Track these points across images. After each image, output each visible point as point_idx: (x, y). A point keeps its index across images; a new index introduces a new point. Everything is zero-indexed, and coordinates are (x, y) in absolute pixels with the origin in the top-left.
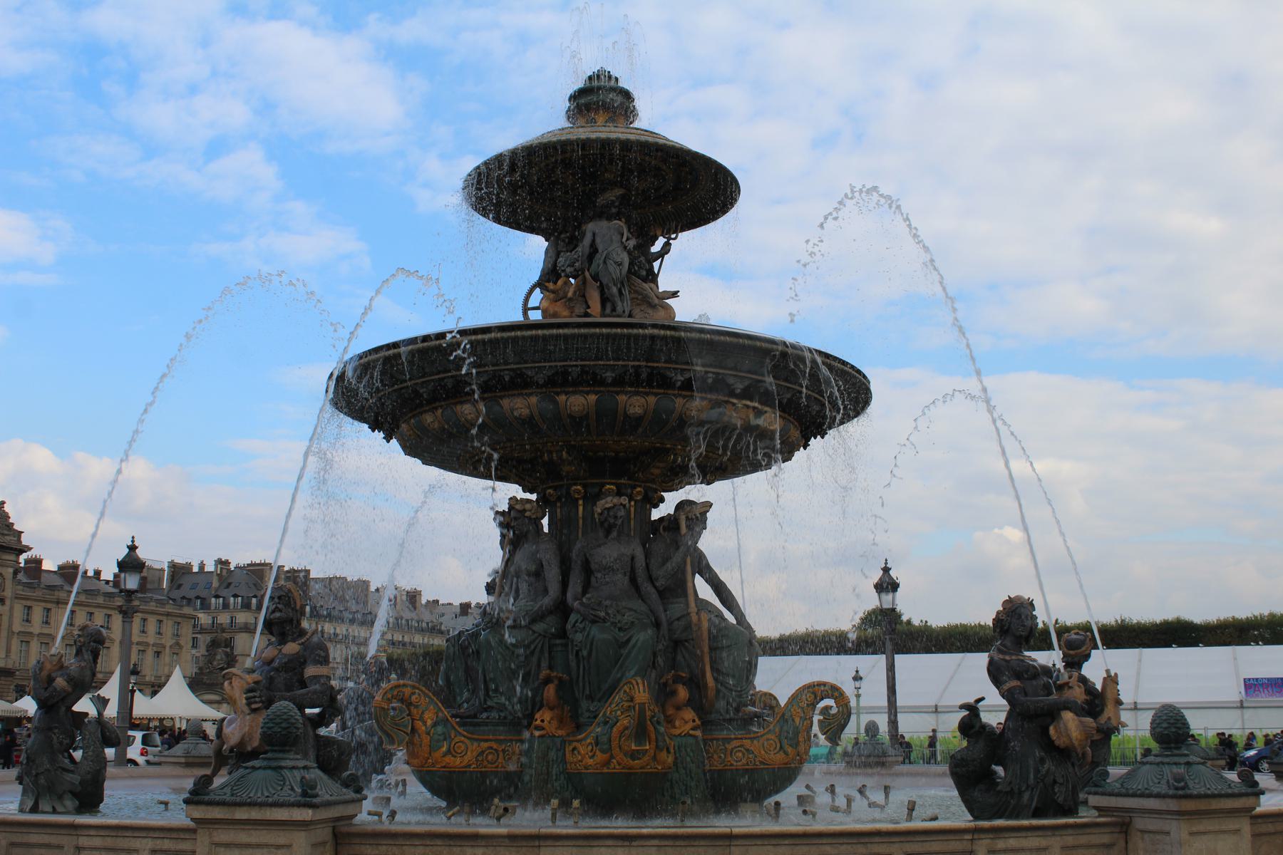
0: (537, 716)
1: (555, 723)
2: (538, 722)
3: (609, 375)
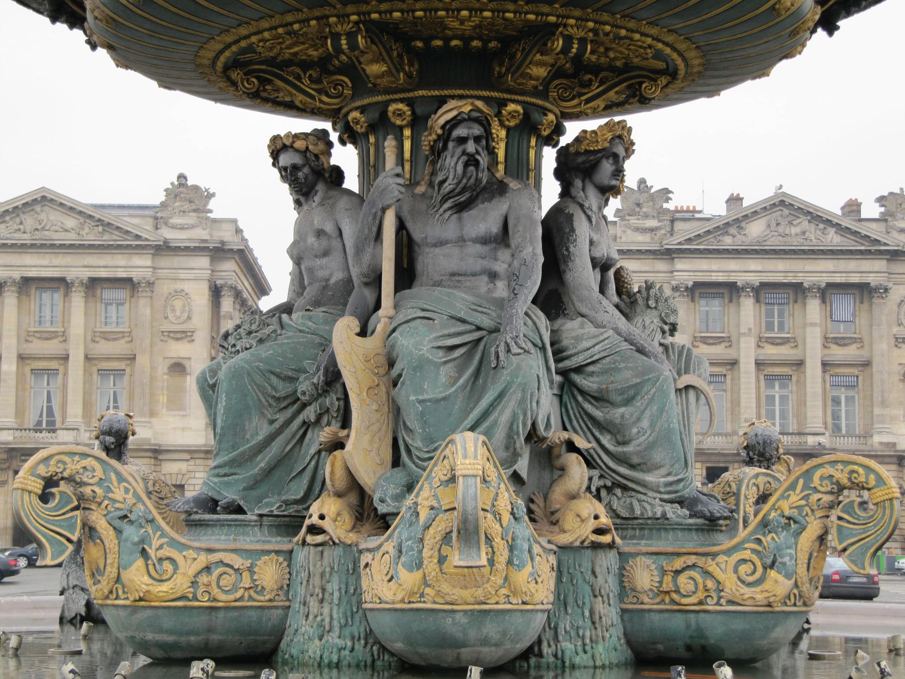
1: (347, 519)
2: (315, 520)
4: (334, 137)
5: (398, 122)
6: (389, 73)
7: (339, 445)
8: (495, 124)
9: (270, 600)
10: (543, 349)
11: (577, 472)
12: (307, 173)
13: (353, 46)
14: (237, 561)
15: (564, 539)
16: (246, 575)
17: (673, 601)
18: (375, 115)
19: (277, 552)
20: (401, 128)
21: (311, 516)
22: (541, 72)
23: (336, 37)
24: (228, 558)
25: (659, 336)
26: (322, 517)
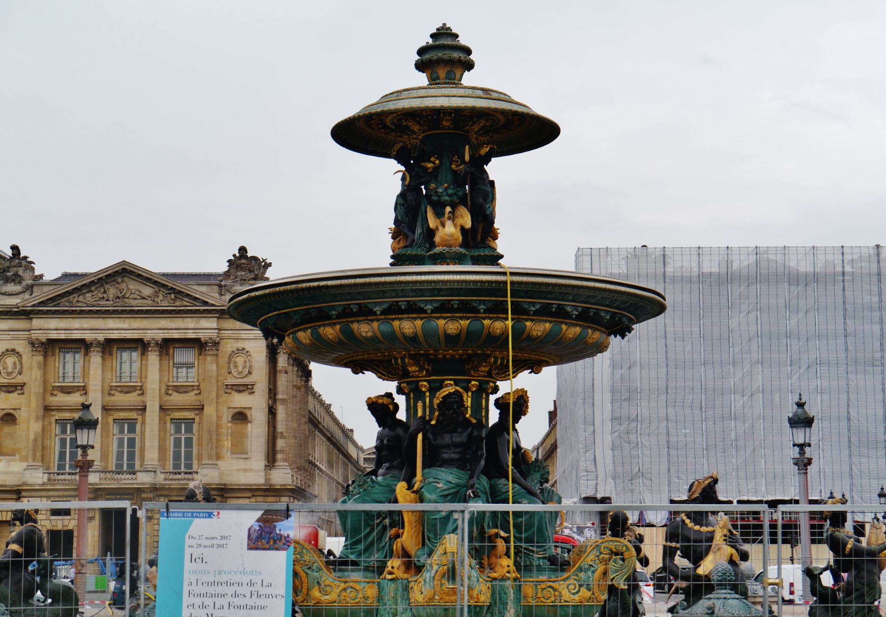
0: (389, 564)
1: (403, 568)
2: (390, 568)
3: (429, 307)
4: (395, 395)
5: (424, 389)
6: (419, 371)
7: (398, 536)
8: (465, 396)
10: (486, 493)
11: (501, 545)
12: (381, 409)
13: (403, 362)
15: (495, 575)
17: (542, 602)
18: (413, 386)
20: (425, 392)
22: (487, 369)
23: (396, 359)
25: (538, 486)
26: (393, 567)
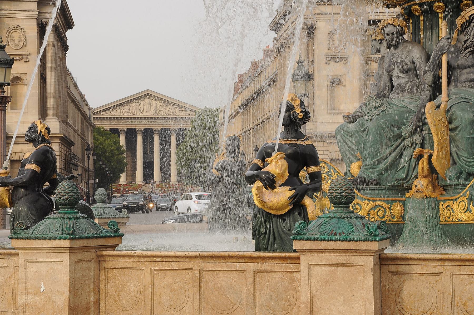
9: (397, 221)
14: (385, 205)
16: (388, 210)
19: (399, 201)
21: (416, 186)
24: (381, 203)
